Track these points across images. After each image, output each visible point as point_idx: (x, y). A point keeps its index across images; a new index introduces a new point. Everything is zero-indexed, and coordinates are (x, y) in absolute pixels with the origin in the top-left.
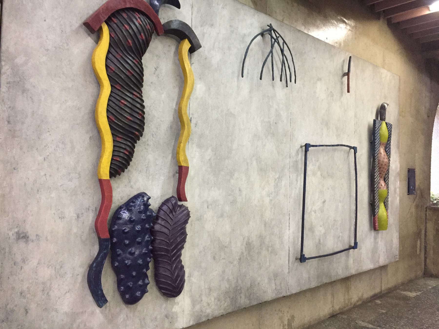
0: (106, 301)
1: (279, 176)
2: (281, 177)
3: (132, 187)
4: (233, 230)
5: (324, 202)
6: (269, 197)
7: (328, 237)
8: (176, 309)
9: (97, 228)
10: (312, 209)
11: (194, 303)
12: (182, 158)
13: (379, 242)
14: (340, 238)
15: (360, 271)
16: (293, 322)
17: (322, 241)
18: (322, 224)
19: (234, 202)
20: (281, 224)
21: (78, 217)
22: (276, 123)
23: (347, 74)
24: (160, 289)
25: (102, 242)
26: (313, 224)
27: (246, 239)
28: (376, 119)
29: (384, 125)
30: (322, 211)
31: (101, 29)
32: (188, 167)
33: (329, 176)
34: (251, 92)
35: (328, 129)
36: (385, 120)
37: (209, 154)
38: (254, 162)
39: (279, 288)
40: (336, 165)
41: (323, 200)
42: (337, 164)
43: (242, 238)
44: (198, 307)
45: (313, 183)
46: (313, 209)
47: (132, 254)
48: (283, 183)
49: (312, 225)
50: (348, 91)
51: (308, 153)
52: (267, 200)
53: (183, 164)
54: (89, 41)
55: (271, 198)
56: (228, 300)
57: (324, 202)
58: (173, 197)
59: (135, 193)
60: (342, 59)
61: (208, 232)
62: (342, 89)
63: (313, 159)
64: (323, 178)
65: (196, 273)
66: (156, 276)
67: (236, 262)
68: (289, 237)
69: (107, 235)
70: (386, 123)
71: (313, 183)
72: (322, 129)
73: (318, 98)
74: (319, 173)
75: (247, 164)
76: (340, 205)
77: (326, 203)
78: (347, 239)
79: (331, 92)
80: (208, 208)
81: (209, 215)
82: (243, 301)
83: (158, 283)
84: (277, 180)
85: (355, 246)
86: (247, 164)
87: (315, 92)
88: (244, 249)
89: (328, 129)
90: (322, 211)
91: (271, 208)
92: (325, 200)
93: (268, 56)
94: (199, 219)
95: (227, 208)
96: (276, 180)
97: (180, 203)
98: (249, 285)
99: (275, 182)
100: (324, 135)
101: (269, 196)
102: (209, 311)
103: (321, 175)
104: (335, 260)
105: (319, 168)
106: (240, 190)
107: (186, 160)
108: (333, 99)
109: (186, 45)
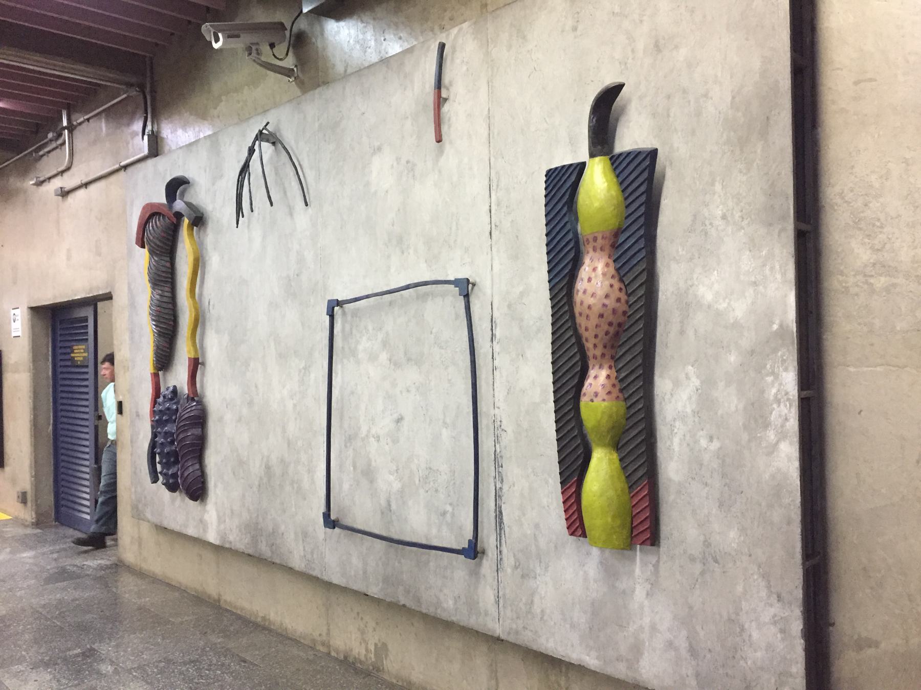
1: (306, 365)
2: (309, 367)
4: (251, 442)
5: (399, 420)
6: (293, 399)
7: (410, 503)
10: (369, 431)
13: (640, 593)
14: (448, 516)
16: (386, 659)
17: (394, 507)
18: (395, 469)
19: (251, 403)
20: (312, 449)
22: (297, 275)
26: (373, 464)
27: (265, 460)
30: (395, 441)
33: (409, 360)
34: (264, 237)
35: (403, 253)
37: (226, 337)
38: (272, 344)
39: (309, 556)
40: (431, 333)
41: (396, 416)
42: (434, 331)
43: (261, 458)
44: (222, 527)
45: (369, 378)
46: (373, 431)
48: (313, 376)
49: (369, 465)
52: (290, 405)
55: (295, 402)
56: (248, 535)
57: (399, 420)
61: (228, 439)
63: (370, 328)
64: (392, 367)
65: (220, 485)
67: (255, 489)
71: (369, 378)
72: (389, 257)
73: (376, 192)
74: (384, 356)
75: (264, 348)
76: (445, 433)
77: (405, 423)
79: (408, 162)
80: (227, 407)
81: (228, 417)
84: (303, 371)
86: (264, 348)
87: (367, 184)
88: (263, 473)
89: (403, 253)
90: (395, 441)
91: (296, 419)
92: (400, 415)
94: (221, 419)
95: (245, 411)
96: (300, 371)
98: (271, 531)
99: (299, 375)
100: (393, 270)
101: (292, 398)
103: (390, 360)
104: (432, 564)
105: (385, 344)
106: (256, 387)
108: (414, 176)
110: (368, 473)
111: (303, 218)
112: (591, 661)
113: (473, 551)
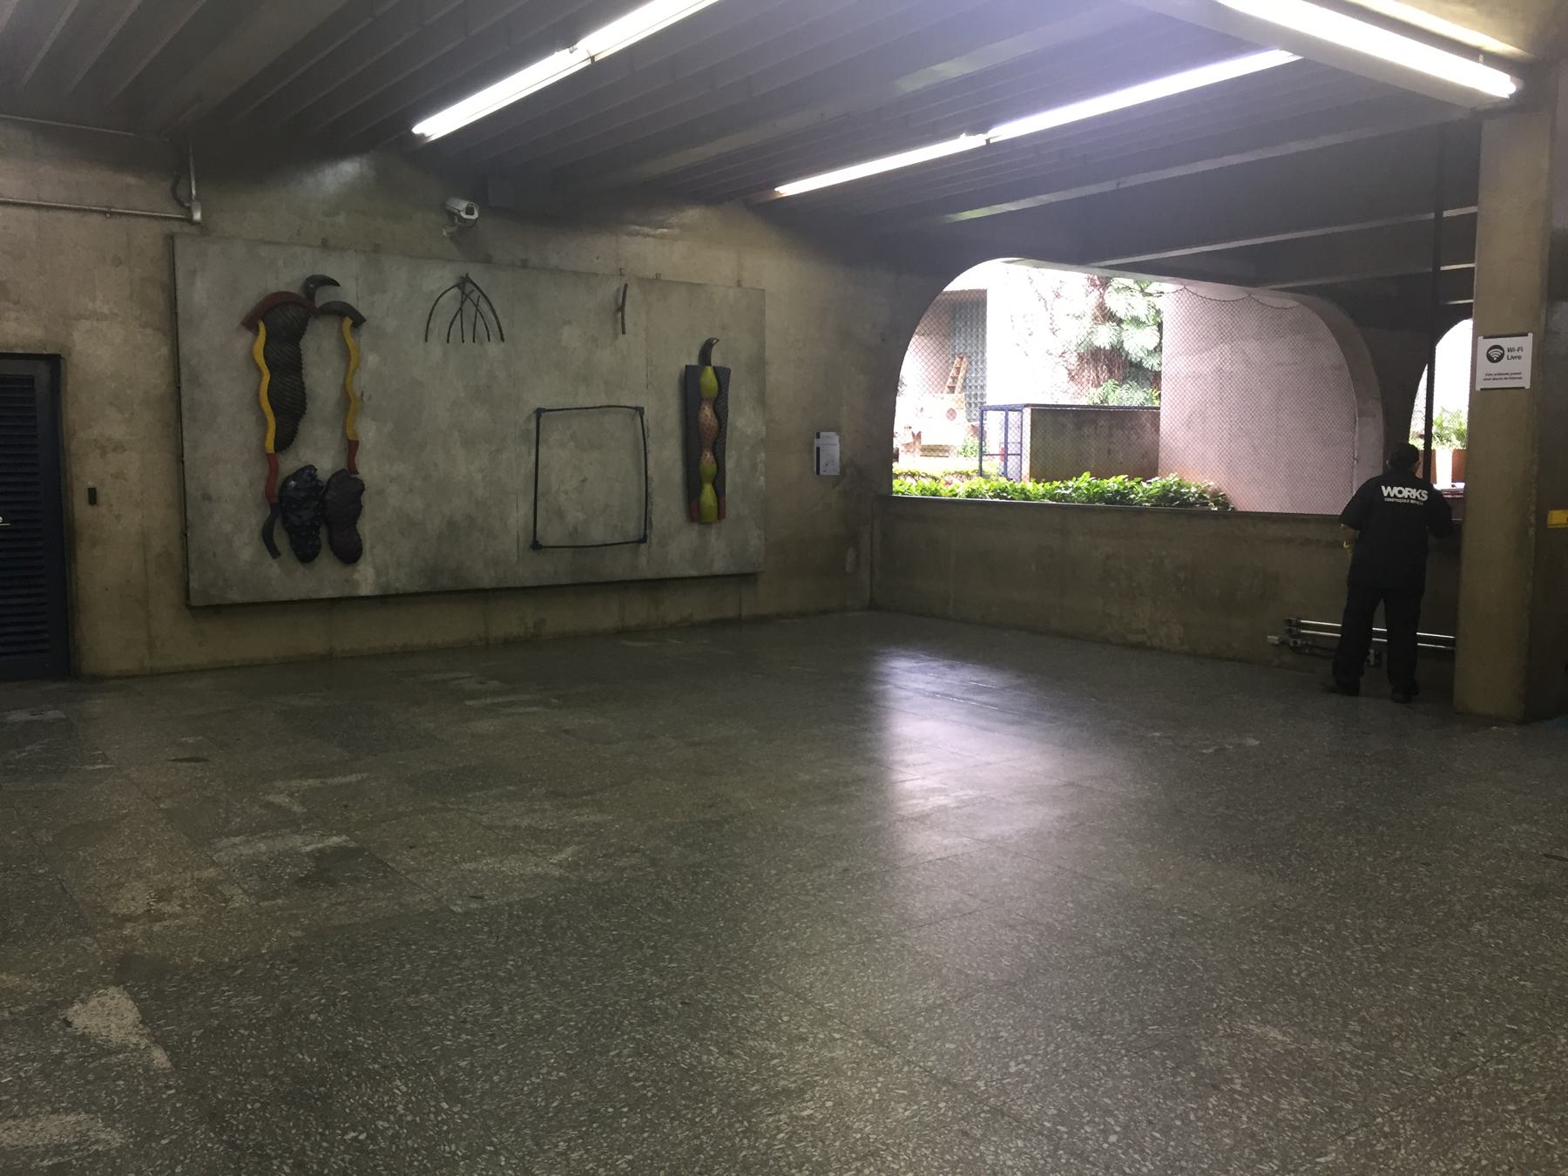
0: (279, 554)
3: (300, 460)
5: (585, 480)
8: (356, 576)
9: (268, 494)
11: (378, 574)
12: (349, 432)
15: (664, 575)
18: (580, 508)
21: (251, 484)
22: (488, 387)
23: (621, 309)
24: (336, 554)
25: (273, 506)
28: (700, 364)
29: (709, 370)
31: (258, 326)
32: (358, 442)
36: (710, 365)
41: (582, 478)
44: (383, 579)
47: (300, 517)
50: (624, 333)
51: (541, 420)
52: (479, 476)
53: (351, 438)
54: (250, 335)
57: (585, 480)
58: (344, 470)
59: (302, 466)
60: (615, 288)
62: (615, 329)
66: (331, 542)
68: (517, 521)
69: (275, 500)
70: (715, 369)
78: (632, 529)
82: (445, 582)
83: (333, 548)
85: (643, 540)
93: (457, 314)
97: (353, 476)
102: (397, 585)
106: (436, 465)
107: (355, 434)
109: (348, 322)
110: (560, 515)
111: (494, 349)
112: (694, 573)
113: (643, 540)
